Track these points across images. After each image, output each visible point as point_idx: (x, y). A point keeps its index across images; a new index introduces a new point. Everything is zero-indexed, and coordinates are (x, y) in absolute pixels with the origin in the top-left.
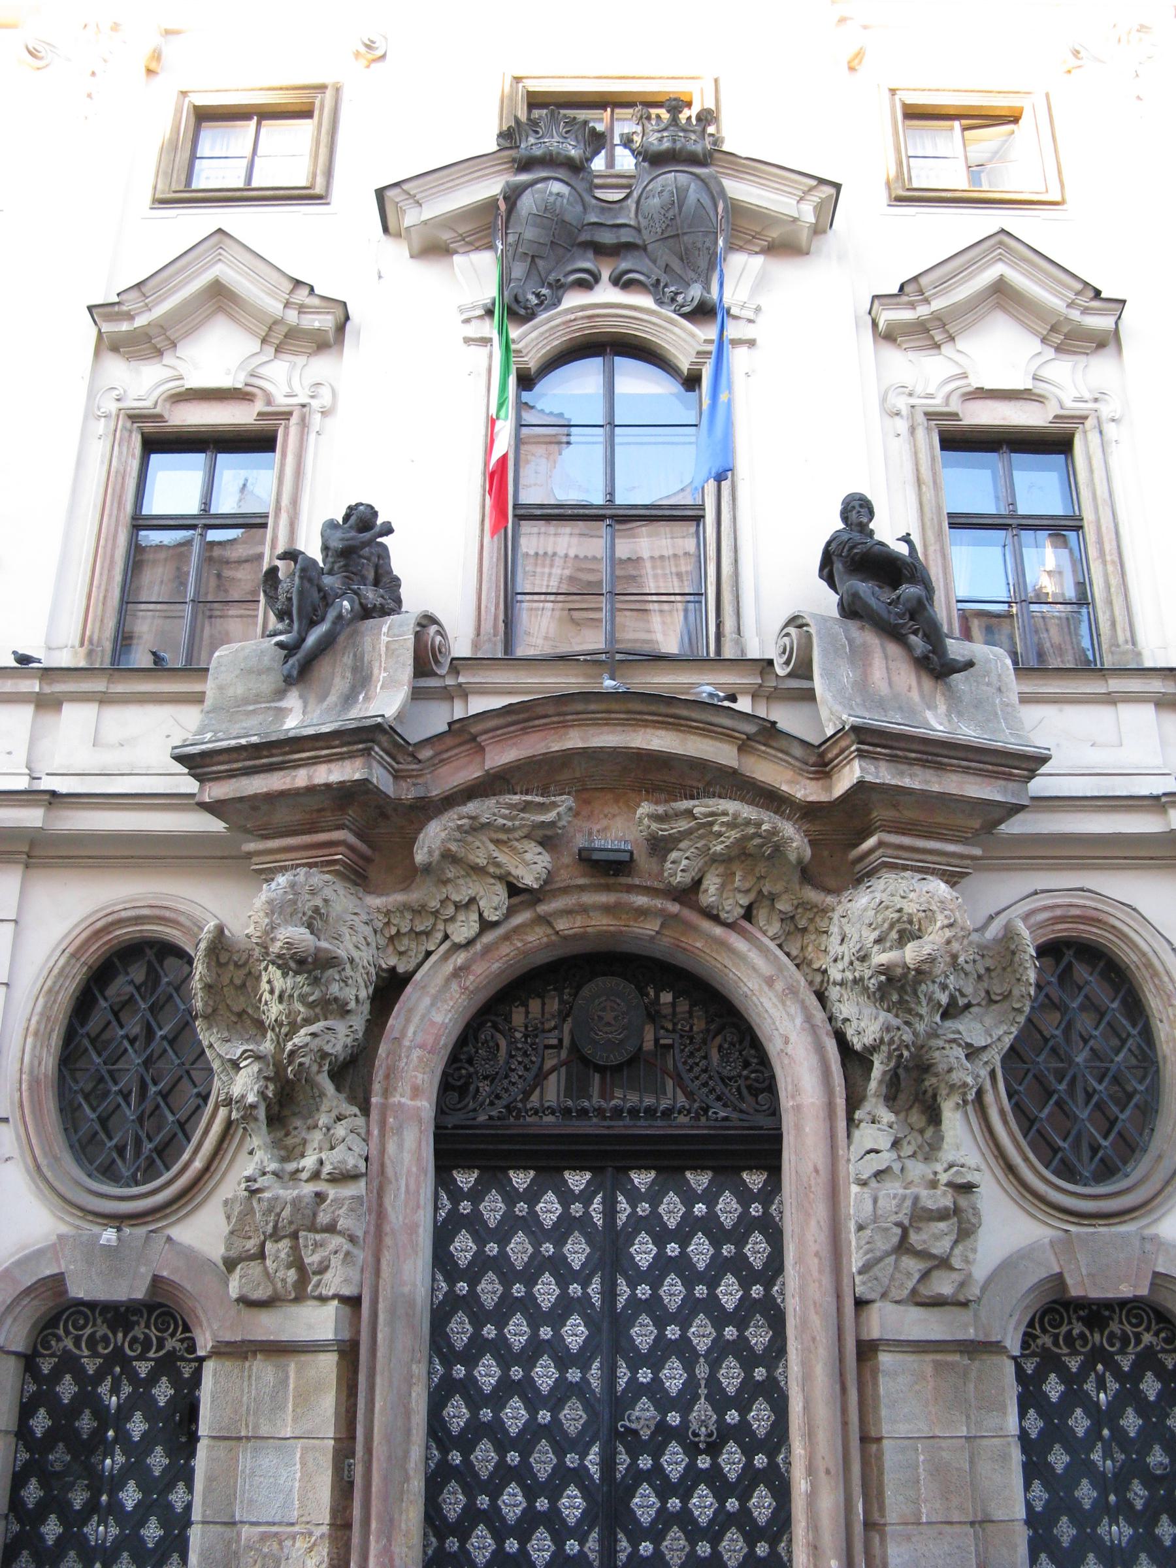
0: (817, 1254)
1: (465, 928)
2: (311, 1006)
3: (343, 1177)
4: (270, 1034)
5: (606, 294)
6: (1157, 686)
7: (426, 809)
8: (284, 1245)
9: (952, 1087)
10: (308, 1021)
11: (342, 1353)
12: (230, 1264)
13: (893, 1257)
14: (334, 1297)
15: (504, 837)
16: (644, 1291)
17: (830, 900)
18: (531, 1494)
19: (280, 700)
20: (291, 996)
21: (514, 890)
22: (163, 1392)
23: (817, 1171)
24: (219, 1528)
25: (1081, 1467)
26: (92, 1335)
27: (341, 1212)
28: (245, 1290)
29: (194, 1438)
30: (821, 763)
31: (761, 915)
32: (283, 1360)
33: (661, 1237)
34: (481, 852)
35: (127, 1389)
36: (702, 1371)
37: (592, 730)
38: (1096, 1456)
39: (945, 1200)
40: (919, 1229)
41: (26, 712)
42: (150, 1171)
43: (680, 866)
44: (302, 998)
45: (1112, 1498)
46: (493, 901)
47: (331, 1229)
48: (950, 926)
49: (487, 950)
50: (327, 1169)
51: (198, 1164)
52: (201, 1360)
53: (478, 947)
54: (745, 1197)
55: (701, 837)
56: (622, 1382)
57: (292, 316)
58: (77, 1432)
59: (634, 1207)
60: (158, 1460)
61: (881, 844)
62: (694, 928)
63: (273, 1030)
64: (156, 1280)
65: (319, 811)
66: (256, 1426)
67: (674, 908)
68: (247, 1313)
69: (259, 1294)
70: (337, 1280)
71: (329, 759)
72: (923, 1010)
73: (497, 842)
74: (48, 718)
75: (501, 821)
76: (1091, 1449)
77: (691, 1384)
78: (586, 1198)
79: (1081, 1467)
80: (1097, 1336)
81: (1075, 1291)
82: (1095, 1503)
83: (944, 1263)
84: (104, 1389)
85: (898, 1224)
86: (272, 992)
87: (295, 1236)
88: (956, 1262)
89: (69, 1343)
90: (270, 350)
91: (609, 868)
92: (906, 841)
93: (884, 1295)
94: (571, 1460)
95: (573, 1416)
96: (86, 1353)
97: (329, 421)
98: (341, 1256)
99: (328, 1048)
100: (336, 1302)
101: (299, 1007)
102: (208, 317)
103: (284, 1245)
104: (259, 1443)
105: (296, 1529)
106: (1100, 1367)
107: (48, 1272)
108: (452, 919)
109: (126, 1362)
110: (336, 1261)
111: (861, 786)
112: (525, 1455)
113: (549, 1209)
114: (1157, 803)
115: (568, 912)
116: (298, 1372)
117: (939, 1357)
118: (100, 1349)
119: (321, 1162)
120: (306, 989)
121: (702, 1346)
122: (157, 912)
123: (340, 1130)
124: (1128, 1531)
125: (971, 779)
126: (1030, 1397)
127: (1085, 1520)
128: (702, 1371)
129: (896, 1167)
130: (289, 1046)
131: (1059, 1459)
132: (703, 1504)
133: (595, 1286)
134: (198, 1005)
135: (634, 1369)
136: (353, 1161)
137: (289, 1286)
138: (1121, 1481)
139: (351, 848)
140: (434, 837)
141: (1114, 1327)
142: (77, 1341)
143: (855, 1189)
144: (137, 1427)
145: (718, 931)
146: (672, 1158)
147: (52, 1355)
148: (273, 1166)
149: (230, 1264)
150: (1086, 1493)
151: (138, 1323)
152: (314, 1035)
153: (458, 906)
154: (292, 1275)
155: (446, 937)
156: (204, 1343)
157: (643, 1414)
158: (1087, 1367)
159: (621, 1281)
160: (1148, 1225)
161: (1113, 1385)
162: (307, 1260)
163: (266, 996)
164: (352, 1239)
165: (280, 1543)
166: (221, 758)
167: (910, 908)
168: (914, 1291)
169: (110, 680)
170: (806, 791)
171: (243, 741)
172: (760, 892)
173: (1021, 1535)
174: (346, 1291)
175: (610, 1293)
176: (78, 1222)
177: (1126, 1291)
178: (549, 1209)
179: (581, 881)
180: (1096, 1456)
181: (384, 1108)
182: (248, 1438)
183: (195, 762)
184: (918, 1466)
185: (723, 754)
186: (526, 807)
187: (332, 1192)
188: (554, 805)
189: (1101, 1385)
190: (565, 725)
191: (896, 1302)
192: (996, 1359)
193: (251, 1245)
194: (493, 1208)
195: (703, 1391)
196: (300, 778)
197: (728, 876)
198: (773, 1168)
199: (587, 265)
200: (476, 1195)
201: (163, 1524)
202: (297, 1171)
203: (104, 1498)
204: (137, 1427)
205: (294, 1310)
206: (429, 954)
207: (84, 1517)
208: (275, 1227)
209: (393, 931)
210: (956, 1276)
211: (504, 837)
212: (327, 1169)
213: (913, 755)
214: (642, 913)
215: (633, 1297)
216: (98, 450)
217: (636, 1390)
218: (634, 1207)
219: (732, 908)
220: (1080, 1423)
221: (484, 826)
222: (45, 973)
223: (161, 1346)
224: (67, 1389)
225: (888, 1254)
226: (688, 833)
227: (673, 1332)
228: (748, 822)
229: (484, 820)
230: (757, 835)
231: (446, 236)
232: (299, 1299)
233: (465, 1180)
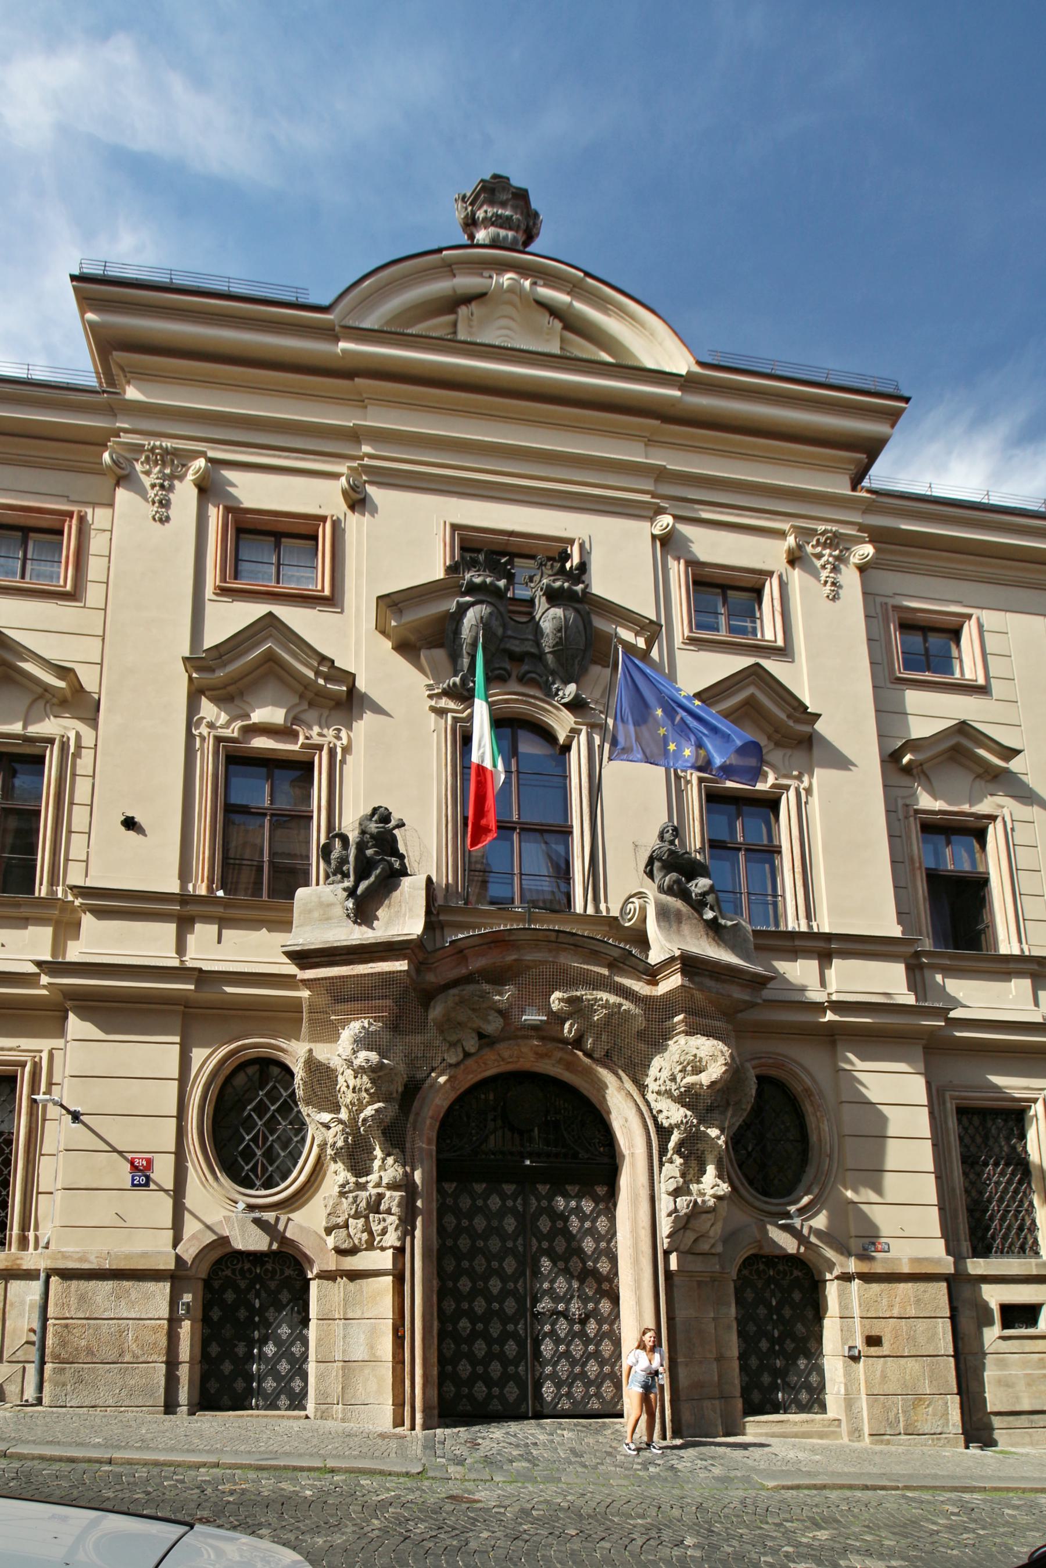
4: (343, 1110)
8: (362, 1220)
10: (369, 1103)
11: (394, 1276)
14: (390, 1247)
20: (360, 1089)
21: (481, 1036)
26: (242, 1269)
29: (305, 1322)
44: (366, 1090)
45: (777, 1348)
47: (389, 1212)
50: (385, 1181)
51: (302, 1178)
52: (311, 1279)
63: (347, 1106)
66: (345, 1313)
69: (345, 1246)
82: (769, 1349)
84: (251, 1296)
86: (348, 1087)
87: (367, 1217)
89: (228, 1272)
98: (394, 1226)
100: (391, 1250)
101: (364, 1094)
103: (362, 1220)
106: (772, 1287)
110: (391, 1229)
118: (247, 1275)
119: (381, 1177)
120: (369, 1085)
123: (390, 1160)
126: (740, 1302)
130: (362, 1116)
134: (300, 1093)
137: (363, 1242)
138: (781, 1341)
142: (234, 1271)
147: (220, 1279)
148: (353, 1179)
149: (329, 1231)
150: (764, 1345)
154: (365, 1236)
162: (374, 1229)
163: (344, 1089)
173: (736, 1364)
187: (388, 1194)
193: (340, 1221)
201: (289, 1362)
202: (367, 1182)
212: (385, 1181)
224: (230, 1296)
232: (370, 1246)
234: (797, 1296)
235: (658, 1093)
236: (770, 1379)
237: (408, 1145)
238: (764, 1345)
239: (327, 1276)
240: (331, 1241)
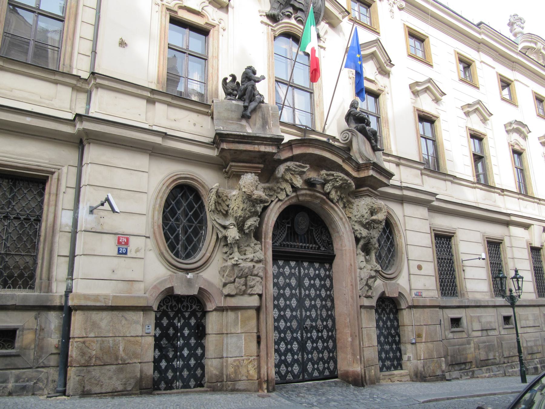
0: (352, 285)
2: (251, 213)
3: (259, 261)
9: (375, 248)
12: (225, 285)
15: (293, 173)
17: (353, 201)
18: (286, 344)
19: (240, 121)
20: (246, 209)
22: (193, 321)
23: (351, 265)
24: (219, 360)
27: (260, 271)
28: (229, 292)
30: (359, 167)
31: (340, 202)
32: (237, 312)
33: (310, 279)
34: (288, 176)
35: (182, 321)
36: (319, 312)
37: (314, 149)
41: (144, 102)
42: (188, 256)
46: (289, 189)
47: (256, 275)
54: (326, 270)
58: (169, 334)
59: (304, 271)
60: (193, 341)
61: (368, 190)
62: (327, 203)
65: (254, 157)
66: (231, 330)
67: (325, 197)
68: (228, 298)
69: (233, 293)
70: (258, 290)
71: (265, 145)
73: (291, 174)
74: (151, 106)
75: (294, 169)
77: (317, 315)
81: (387, 295)
84: (176, 321)
87: (246, 277)
91: (310, 184)
94: (295, 335)
95: (295, 324)
96: (170, 310)
97: (225, 33)
98: (259, 283)
103: (244, 279)
104: (232, 335)
105: (244, 358)
107: (168, 286)
108: (279, 193)
109: (182, 313)
111: (372, 176)
112: (285, 334)
113: (287, 270)
115: (303, 195)
116: (241, 315)
121: (319, 306)
122: (192, 177)
128: (319, 312)
132: (320, 345)
133: (297, 291)
136: (262, 257)
141: (386, 303)
142: (167, 306)
143: (358, 270)
144: (186, 332)
145: (332, 205)
146: (312, 259)
149: (225, 285)
151: (184, 301)
153: (282, 190)
155: (277, 197)
156: (210, 306)
157: (308, 322)
158: (382, 311)
159: (302, 290)
164: (262, 278)
165: (239, 362)
166: (231, 136)
167: (375, 206)
169: (172, 99)
170: (355, 174)
171: (242, 134)
172: (341, 197)
174: (260, 292)
176: (174, 271)
179: (306, 187)
180: (384, 331)
181: (265, 242)
182: (227, 334)
188: (306, 167)
193: (232, 279)
194: (287, 270)
196: (256, 148)
197: (336, 192)
198: (331, 264)
200: (283, 267)
201: (195, 360)
203: (178, 353)
204: (186, 332)
205: (241, 297)
206: (272, 201)
207: (172, 360)
208: (242, 275)
211: (293, 173)
212: (256, 259)
214: (318, 197)
217: (307, 317)
218: (304, 271)
221: (291, 170)
222: (158, 191)
223: (191, 308)
226: (331, 180)
228: (345, 180)
230: (346, 183)
233: (281, 263)
234: (392, 316)
235: (356, 222)
237: (263, 240)
239: (221, 309)
240: (226, 291)
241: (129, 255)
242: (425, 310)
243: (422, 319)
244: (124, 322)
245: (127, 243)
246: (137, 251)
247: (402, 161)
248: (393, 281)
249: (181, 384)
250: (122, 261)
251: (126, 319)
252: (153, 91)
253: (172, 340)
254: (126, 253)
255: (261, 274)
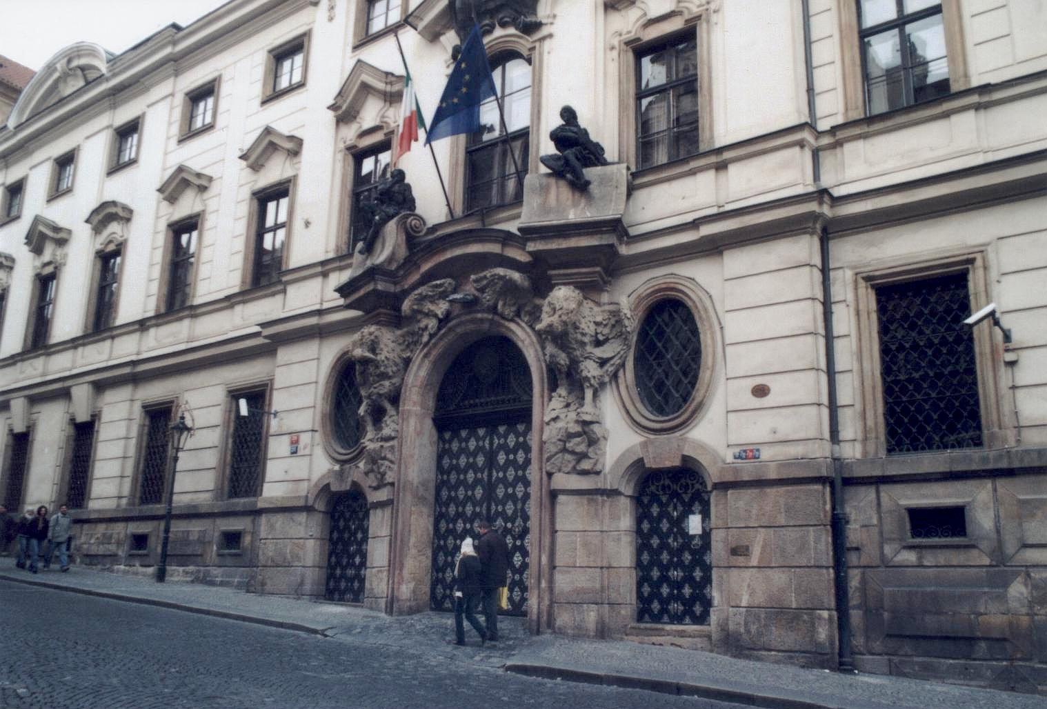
1: (425, 339)
5: (499, 32)
6: (713, 159)
7: (405, 293)
13: (560, 455)
16: (501, 475)
25: (664, 546)
35: (357, 523)
36: (519, 506)
38: (670, 541)
39: (578, 428)
40: (570, 442)
41: (320, 279)
43: (487, 298)
48: (561, 309)
49: (435, 345)
53: (431, 344)
55: (492, 286)
56: (493, 512)
57: (389, 88)
64: (354, 484)
72: (575, 346)
73: (431, 302)
76: (669, 537)
77: (515, 511)
78: (483, 439)
79: (664, 546)
80: (675, 487)
83: (583, 456)
85: (560, 440)
88: (591, 455)
90: (388, 104)
92: (562, 272)
93: (560, 470)
99: (381, 392)
102: (366, 97)
113: (472, 444)
114: (695, 224)
117: (591, 497)
124: (681, 574)
125: (582, 238)
127: (664, 568)
128: (519, 506)
129: (562, 416)
131: (655, 542)
135: (497, 506)
138: (680, 551)
139: (385, 314)
140: (406, 306)
150: (665, 557)
152: (375, 388)
158: (671, 499)
160: (687, 432)
161: (680, 508)
168: (574, 468)
169: (340, 262)
175: (490, 476)
177: (668, 464)
178: (472, 444)
180: (670, 541)
183: (343, 290)
184: (576, 543)
185: (495, 248)
186: (437, 286)
189: (675, 508)
190: (444, 250)
191: (568, 473)
192: (619, 497)
195: (519, 514)
199: (487, 22)
209: (406, 343)
210: (591, 461)
213: (550, 234)
214: (482, 320)
215: (497, 477)
216: (339, 165)
219: (509, 312)
220: (665, 525)
225: (556, 453)
227: (510, 490)
229: (424, 294)
231: (438, 29)
236: (668, 590)
238: (665, 557)
241: (298, 454)
242: (768, 490)
243: (754, 512)
244: (291, 524)
245: (297, 442)
246: (305, 448)
247: (727, 155)
248: (678, 434)
249: (352, 597)
250: (294, 461)
251: (294, 521)
252: (323, 263)
253: (347, 544)
254: (296, 452)
255: (389, 456)
